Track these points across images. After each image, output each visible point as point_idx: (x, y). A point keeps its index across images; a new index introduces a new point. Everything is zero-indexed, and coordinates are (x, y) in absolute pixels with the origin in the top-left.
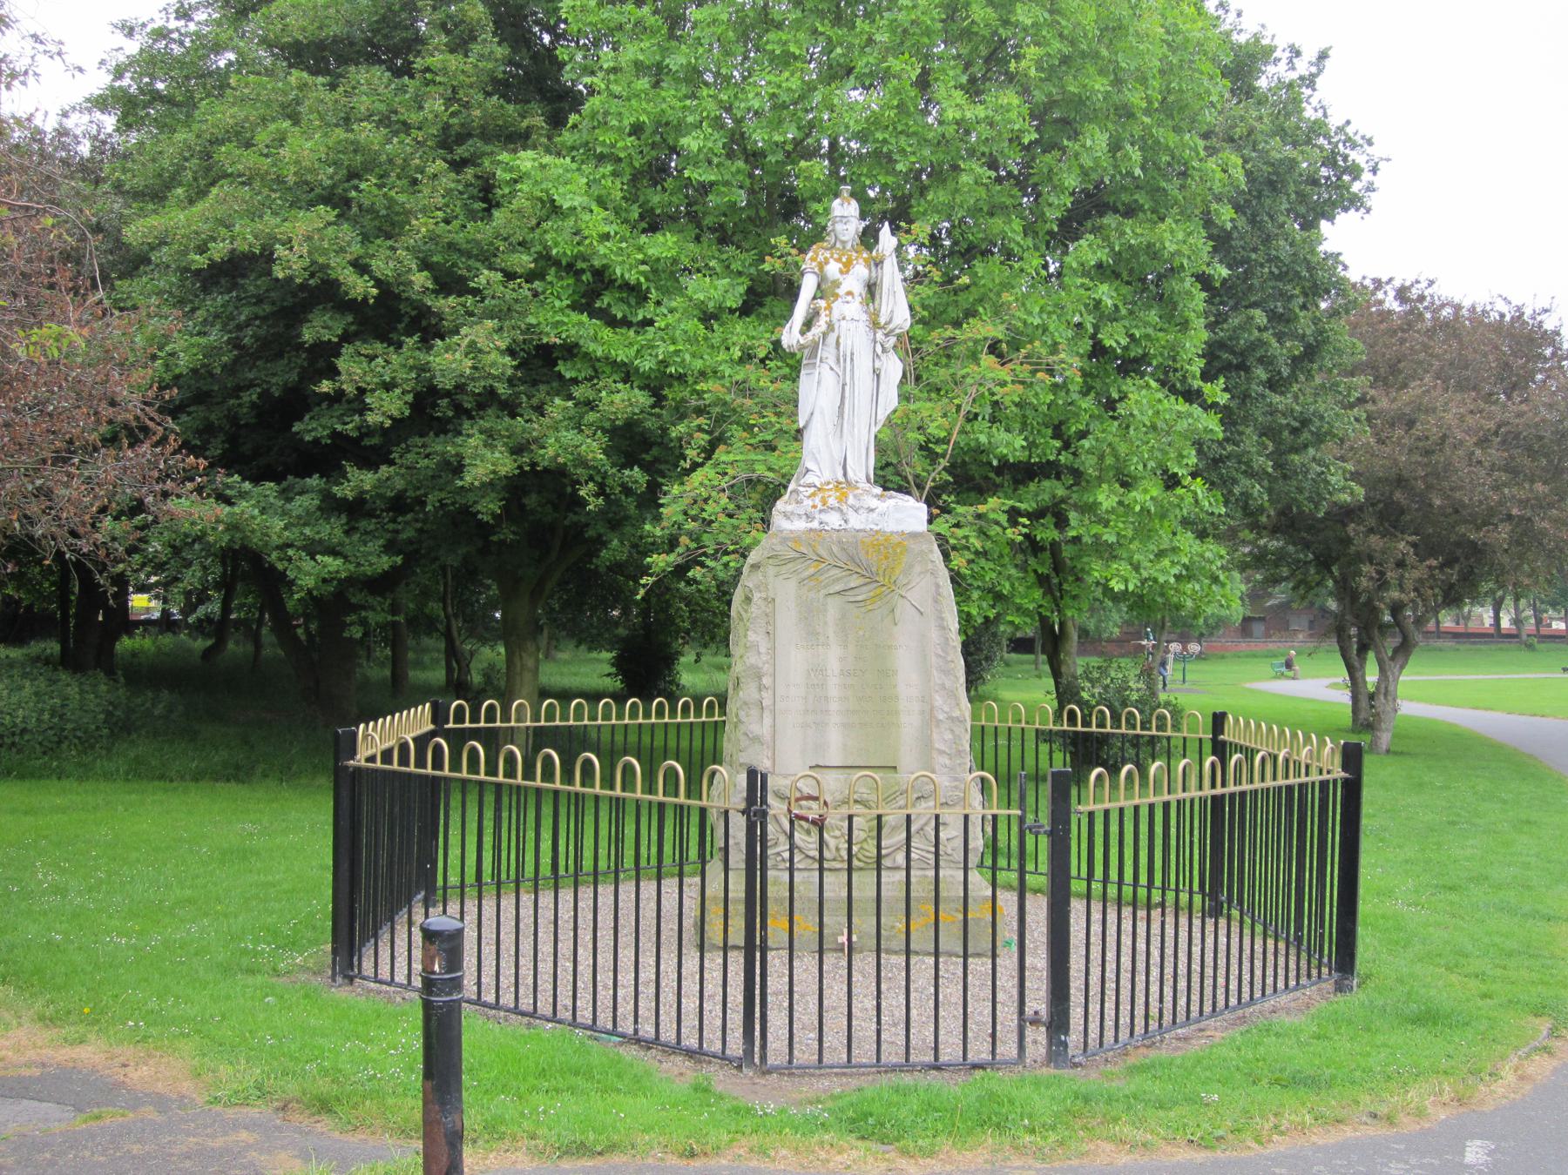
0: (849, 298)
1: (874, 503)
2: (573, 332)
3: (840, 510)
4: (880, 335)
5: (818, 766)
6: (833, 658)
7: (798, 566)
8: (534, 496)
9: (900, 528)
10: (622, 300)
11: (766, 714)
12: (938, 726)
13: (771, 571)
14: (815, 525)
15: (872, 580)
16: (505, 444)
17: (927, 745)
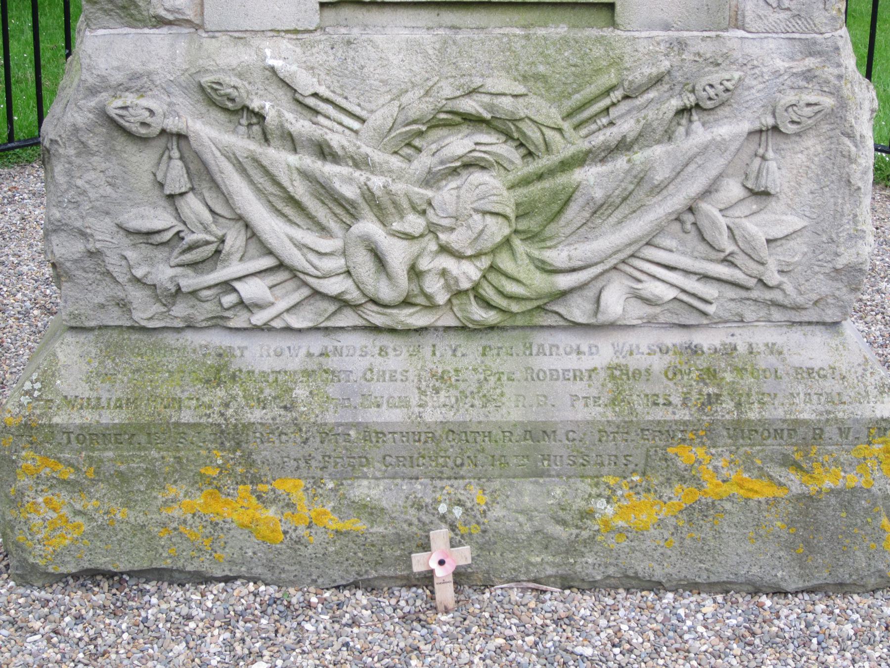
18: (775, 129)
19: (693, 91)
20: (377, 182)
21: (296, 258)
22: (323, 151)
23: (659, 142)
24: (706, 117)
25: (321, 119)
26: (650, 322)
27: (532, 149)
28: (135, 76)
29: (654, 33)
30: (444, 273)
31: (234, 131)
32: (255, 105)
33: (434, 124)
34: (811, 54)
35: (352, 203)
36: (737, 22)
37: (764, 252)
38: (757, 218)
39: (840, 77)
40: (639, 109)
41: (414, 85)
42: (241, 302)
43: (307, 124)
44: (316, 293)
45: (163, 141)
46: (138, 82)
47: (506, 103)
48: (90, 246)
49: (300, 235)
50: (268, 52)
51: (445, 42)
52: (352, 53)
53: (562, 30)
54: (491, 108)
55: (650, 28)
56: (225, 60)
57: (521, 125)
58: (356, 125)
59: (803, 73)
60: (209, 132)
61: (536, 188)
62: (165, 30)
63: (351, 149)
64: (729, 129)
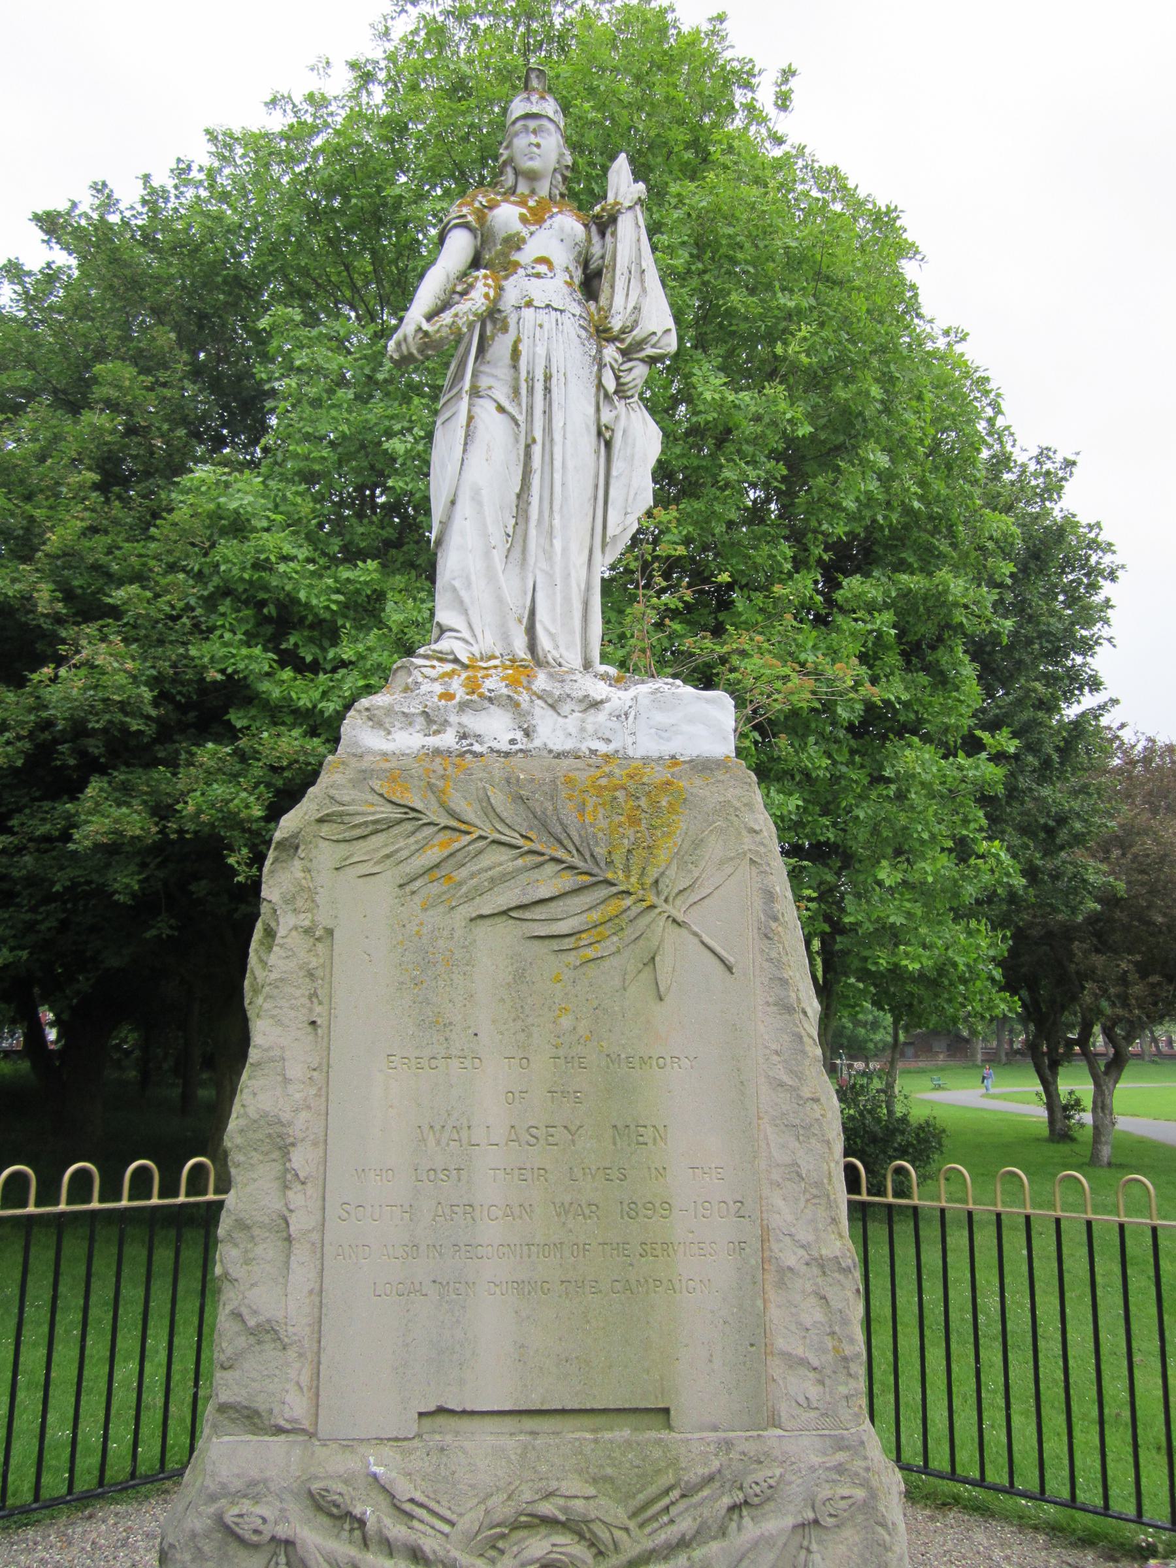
0: (542, 269)
1: (600, 690)
2: (241, 666)
3: (512, 704)
4: (610, 352)
5: (441, 1411)
6: (492, 1092)
7: (399, 841)
8: (204, 882)
9: (667, 748)
10: (311, 640)
11: (301, 1252)
12: (781, 1284)
13: (325, 855)
14: (448, 739)
15: (592, 878)
16: (145, 802)
17: (754, 1343)
18: (816, 1522)
19: (741, 1488)
23: (714, 1538)
24: (755, 1512)
25: (415, 1523)
27: (603, 1549)
28: (253, 1483)
29: (704, 1434)
31: (337, 1536)
32: (357, 1511)
33: (516, 1527)
34: (840, 1449)
36: (774, 1422)
39: (868, 1469)
40: (695, 1506)
41: (498, 1489)
43: (404, 1529)
45: (273, 1545)
46: (254, 1490)
47: (579, 1504)
50: (372, 1459)
51: (526, 1448)
52: (445, 1459)
53: (626, 1433)
54: (565, 1510)
55: (701, 1430)
56: (333, 1467)
57: (591, 1526)
58: (446, 1528)
59: (835, 1467)
62: (282, 1438)
63: (441, 1553)
64: (776, 1524)
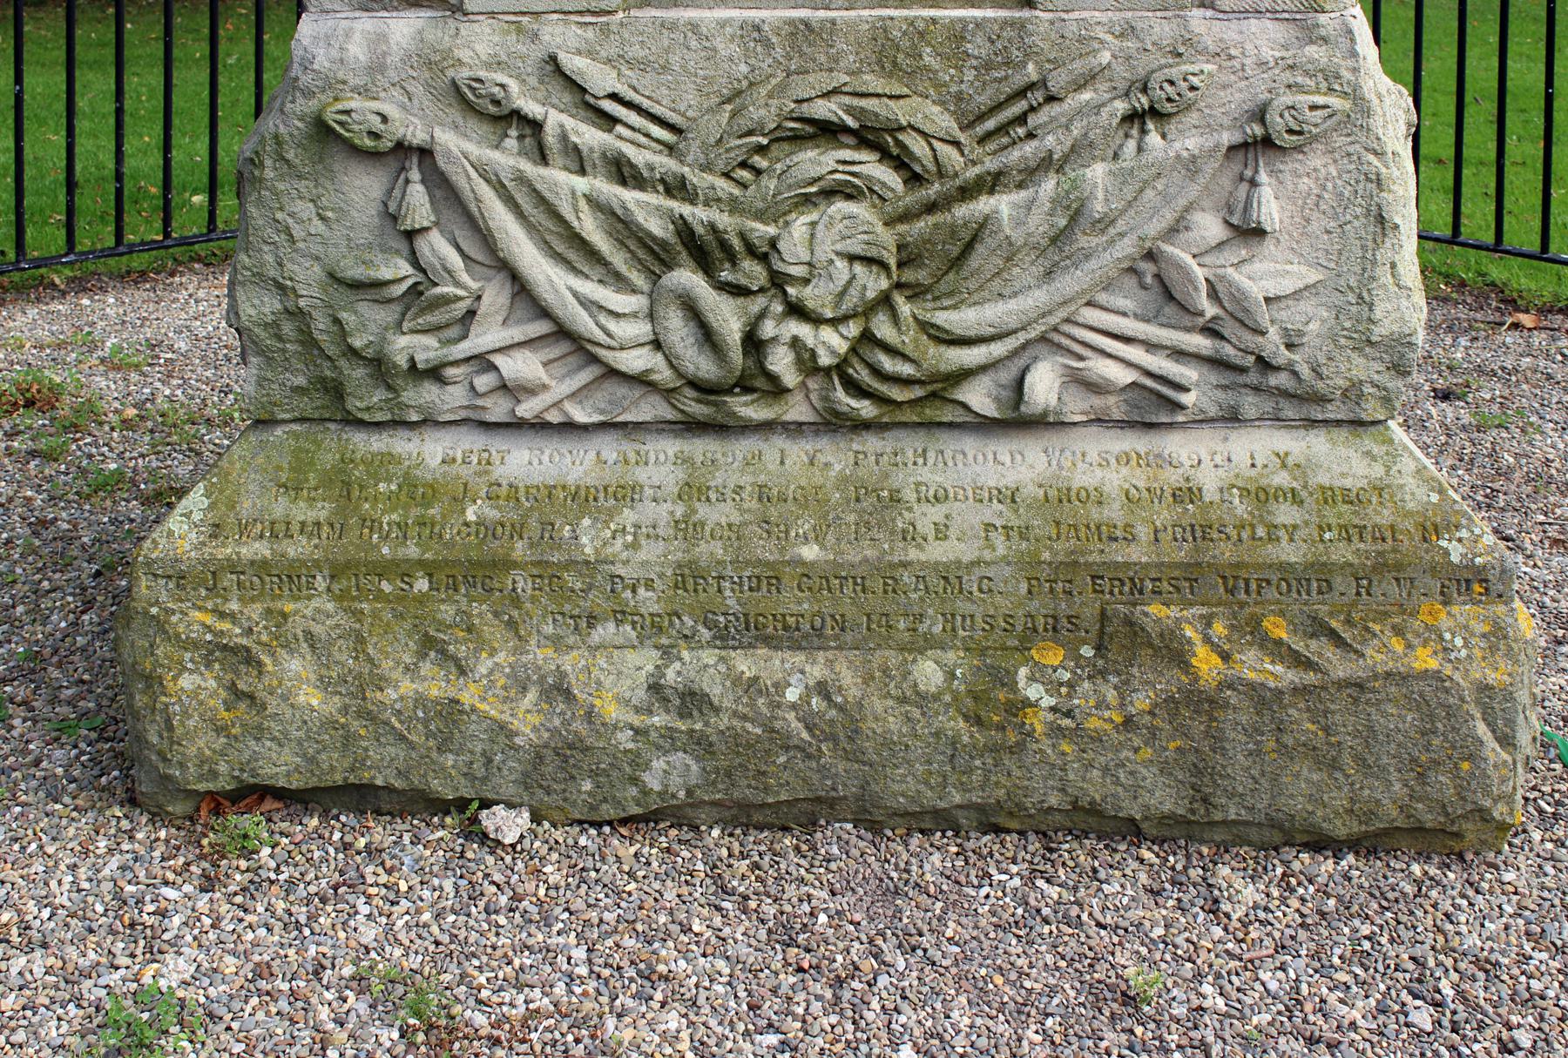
19: (1145, 90)
20: (697, 214)
21: (584, 322)
22: (623, 172)
26: (1099, 420)
27: (918, 169)
30: (795, 343)
35: (663, 244)
37: (1263, 316)
38: (1246, 268)
42: (504, 387)
44: (612, 373)
48: (290, 305)
49: (589, 288)
60: (461, 145)
61: (922, 225)
